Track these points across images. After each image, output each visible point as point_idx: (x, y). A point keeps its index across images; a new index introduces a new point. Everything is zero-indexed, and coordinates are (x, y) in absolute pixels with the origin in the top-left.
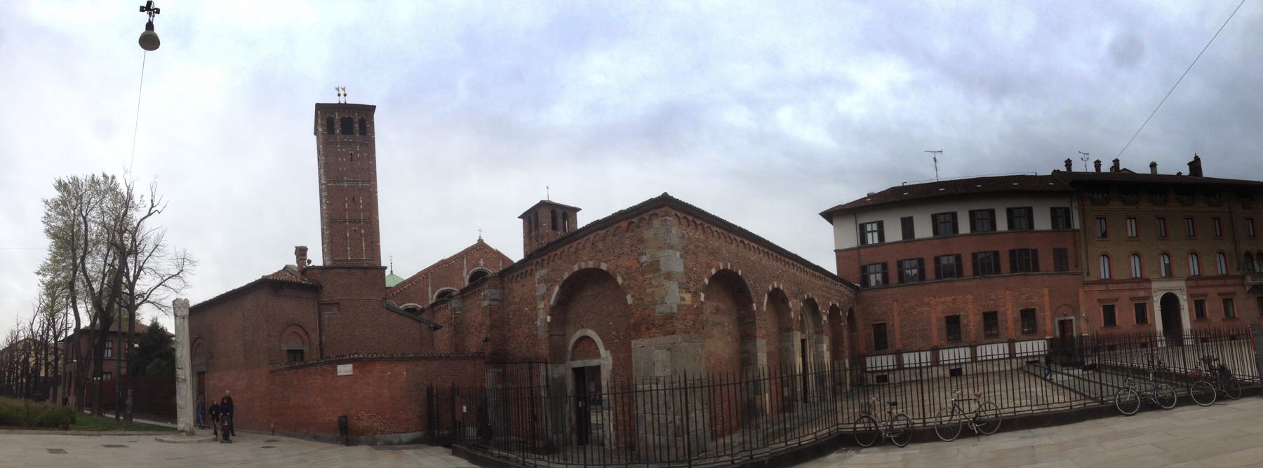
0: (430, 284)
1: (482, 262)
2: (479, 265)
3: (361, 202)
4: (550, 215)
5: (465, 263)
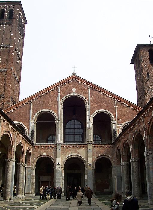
0: (31, 107)
1: (74, 90)
4: (147, 53)
5: (59, 92)
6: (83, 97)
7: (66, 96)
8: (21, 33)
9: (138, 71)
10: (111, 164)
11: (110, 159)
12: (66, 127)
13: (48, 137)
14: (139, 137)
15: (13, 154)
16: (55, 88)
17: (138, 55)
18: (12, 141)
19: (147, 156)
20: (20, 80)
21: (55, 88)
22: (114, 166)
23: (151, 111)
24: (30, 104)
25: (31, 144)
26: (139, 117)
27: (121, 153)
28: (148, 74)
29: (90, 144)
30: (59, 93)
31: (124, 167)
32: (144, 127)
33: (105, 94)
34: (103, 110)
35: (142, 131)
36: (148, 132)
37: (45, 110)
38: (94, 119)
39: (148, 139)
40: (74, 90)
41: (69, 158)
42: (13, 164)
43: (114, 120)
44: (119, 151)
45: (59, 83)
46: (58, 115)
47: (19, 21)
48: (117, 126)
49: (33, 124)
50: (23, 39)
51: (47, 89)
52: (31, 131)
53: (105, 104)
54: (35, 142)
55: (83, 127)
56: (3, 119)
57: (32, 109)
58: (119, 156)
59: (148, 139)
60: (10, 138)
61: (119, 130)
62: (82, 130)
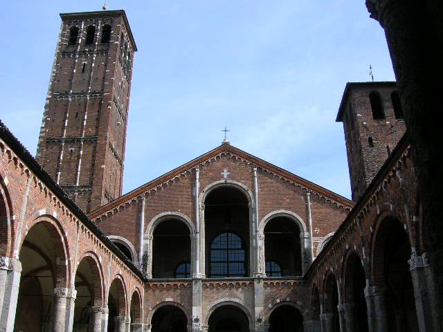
1: (225, 173)
2: (223, 177)
3: (86, 117)
4: (368, 100)
5: (198, 177)
6: (244, 187)
7: (210, 185)
8: (124, 68)
9: (352, 135)
10: (301, 319)
11: (299, 308)
12: (212, 247)
13: (177, 266)
14: (354, 258)
15: (104, 297)
16: (188, 170)
17: (350, 104)
18: (102, 273)
19: (371, 297)
20: (123, 157)
21: (190, 170)
22: (308, 323)
23: (375, 204)
24: (141, 201)
25: (142, 279)
26: (353, 219)
27: (321, 296)
28: (370, 140)
29: (259, 279)
30: (197, 181)
31: (327, 322)
32: (362, 239)
33: (286, 179)
34: (283, 211)
35: (359, 247)
36: (370, 248)
37: (169, 213)
38: (266, 230)
39: (370, 262)
40: (225, 173)
41: (218, 306)
42: (104, 317)
43: (305, 229)
44: (316, 292)
45: (198, 161)
46: (195, 222)
47: (121, 46)
48: (314, 243)
49: (146, 242)
50: (129, 79)
51: (174, 172)
52: (142, 254)
53: (288, 200)
54: (150, 276)
55: (246, 245)
56: (82, 227)
57: (146, 212)
58: (316, 302)
59: (370, 262)
60: (98, 265)
61: (315, 252)
62: (243, 251)
